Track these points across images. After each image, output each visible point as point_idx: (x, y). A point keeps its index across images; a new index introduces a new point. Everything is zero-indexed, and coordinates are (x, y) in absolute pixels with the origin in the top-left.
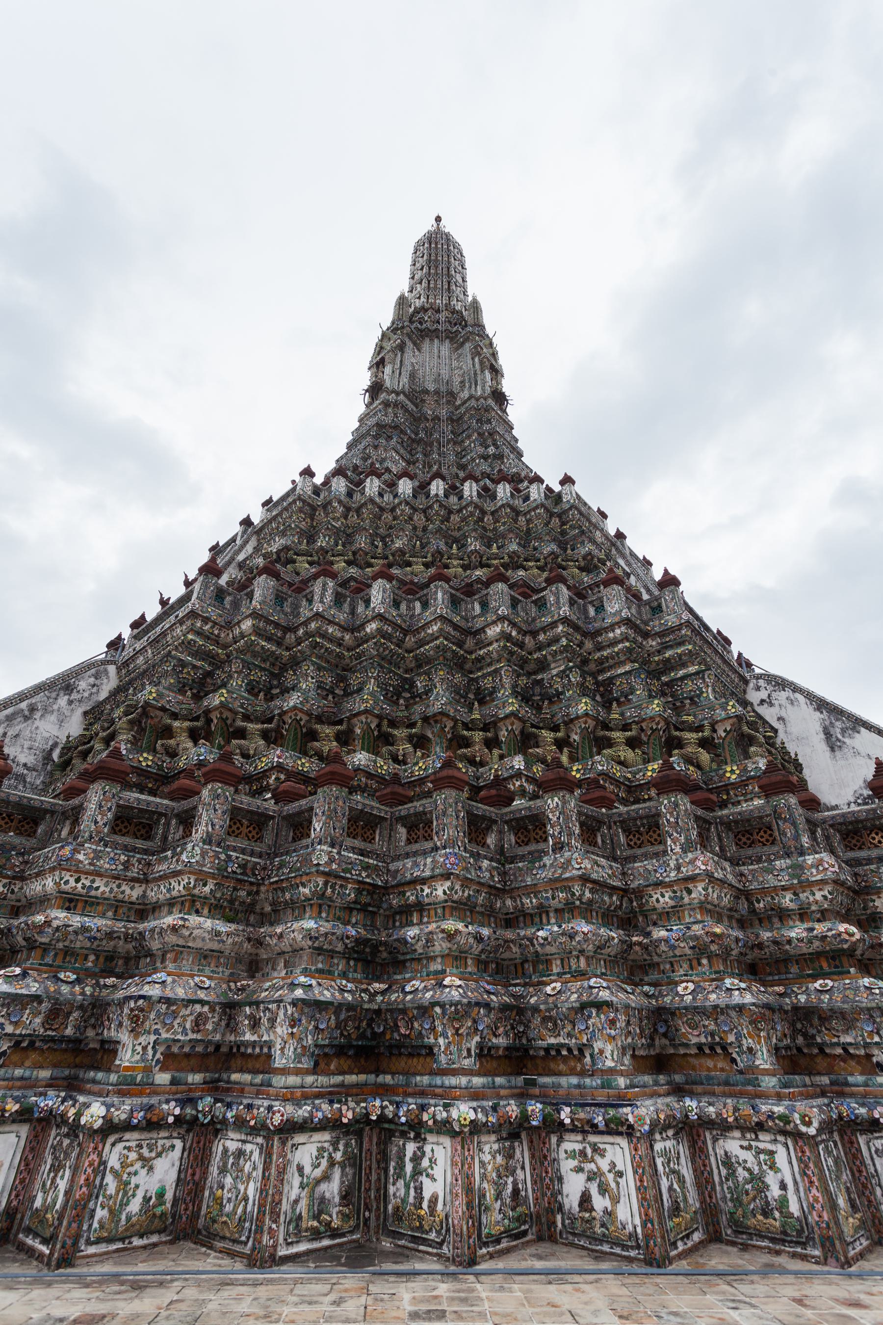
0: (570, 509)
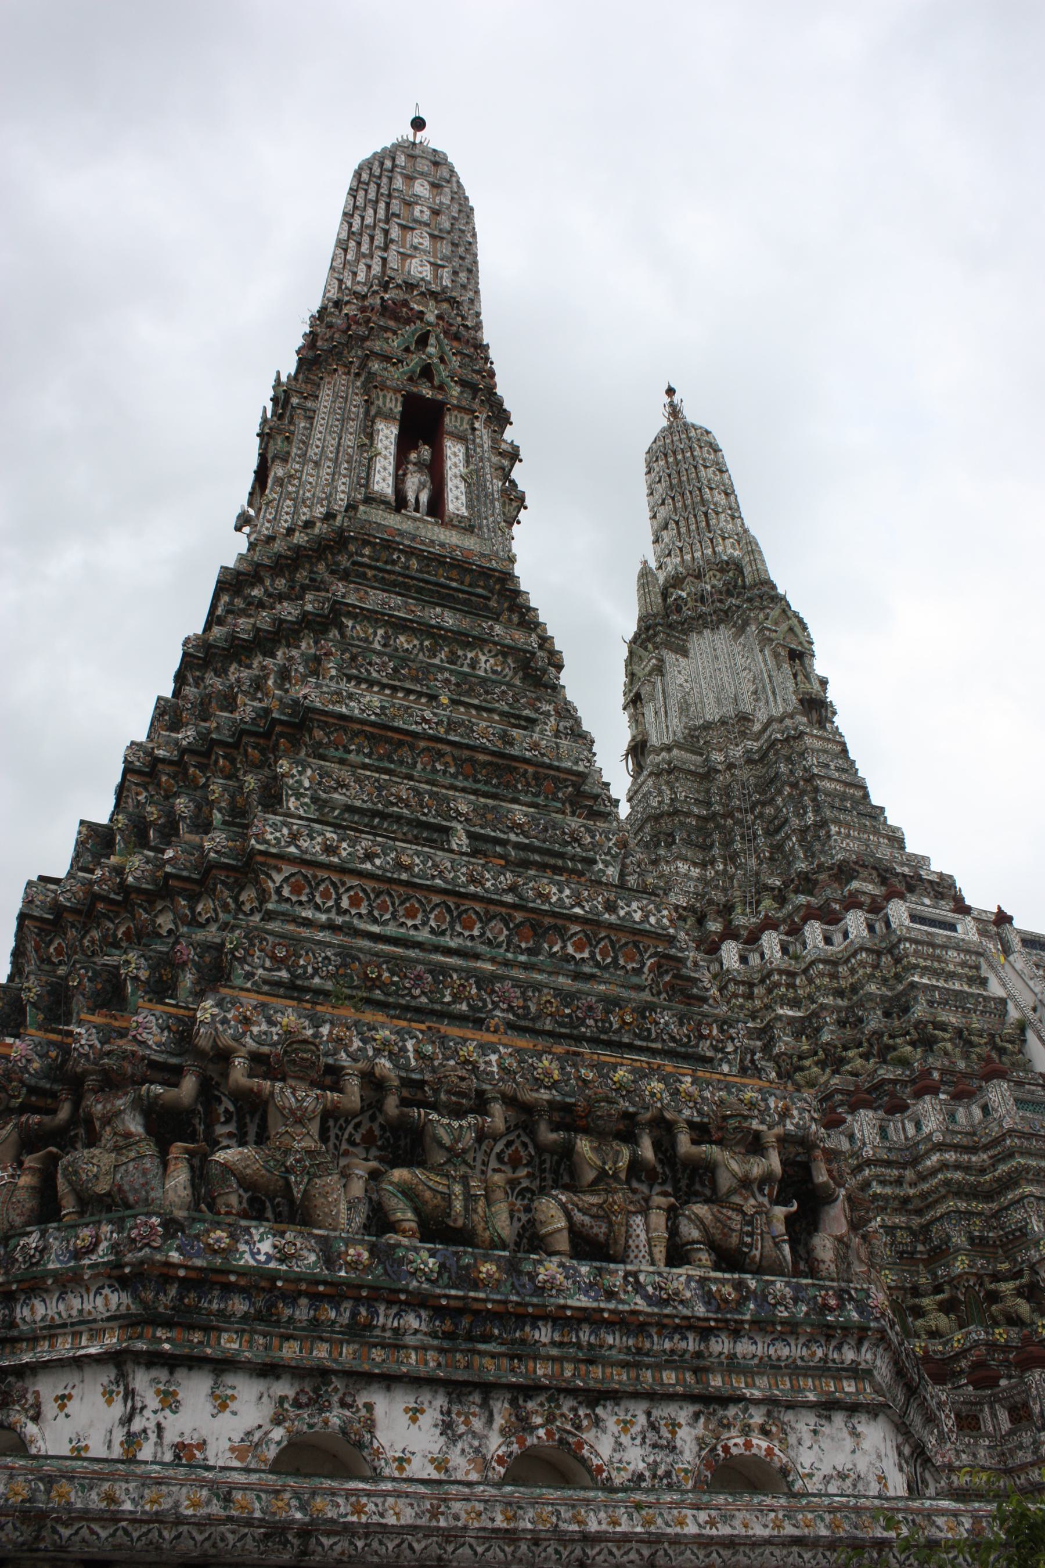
0: (900, 941)
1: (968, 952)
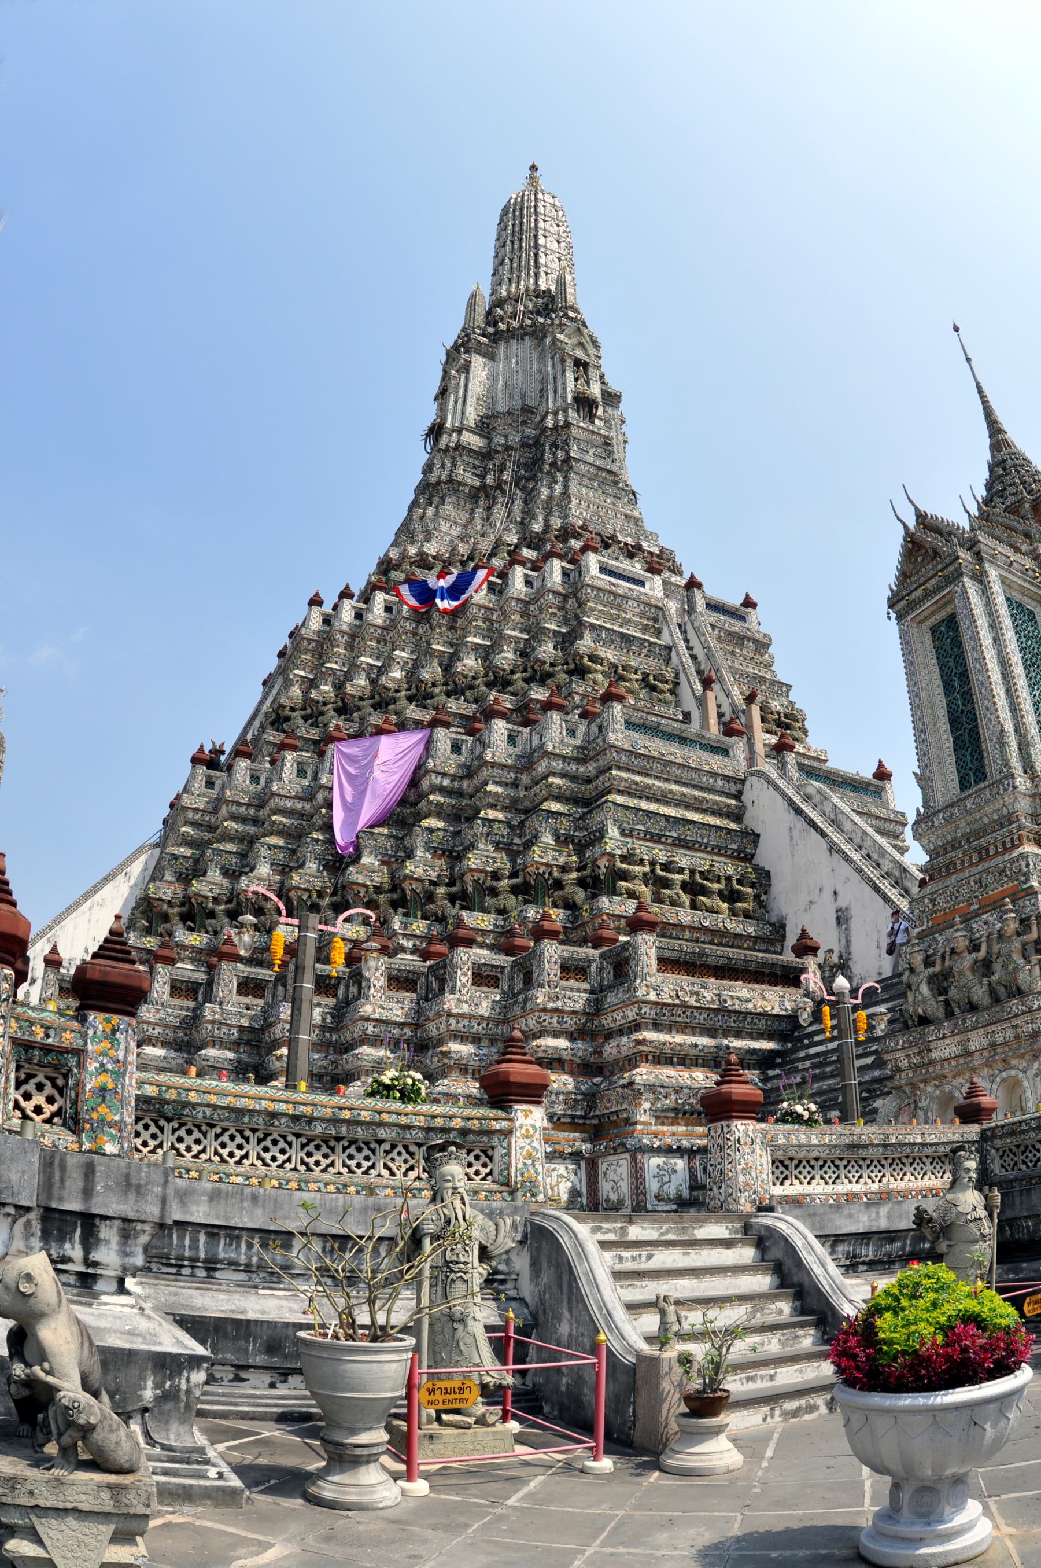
1: (650, 605)
